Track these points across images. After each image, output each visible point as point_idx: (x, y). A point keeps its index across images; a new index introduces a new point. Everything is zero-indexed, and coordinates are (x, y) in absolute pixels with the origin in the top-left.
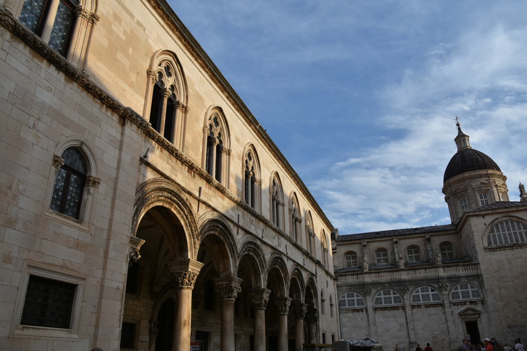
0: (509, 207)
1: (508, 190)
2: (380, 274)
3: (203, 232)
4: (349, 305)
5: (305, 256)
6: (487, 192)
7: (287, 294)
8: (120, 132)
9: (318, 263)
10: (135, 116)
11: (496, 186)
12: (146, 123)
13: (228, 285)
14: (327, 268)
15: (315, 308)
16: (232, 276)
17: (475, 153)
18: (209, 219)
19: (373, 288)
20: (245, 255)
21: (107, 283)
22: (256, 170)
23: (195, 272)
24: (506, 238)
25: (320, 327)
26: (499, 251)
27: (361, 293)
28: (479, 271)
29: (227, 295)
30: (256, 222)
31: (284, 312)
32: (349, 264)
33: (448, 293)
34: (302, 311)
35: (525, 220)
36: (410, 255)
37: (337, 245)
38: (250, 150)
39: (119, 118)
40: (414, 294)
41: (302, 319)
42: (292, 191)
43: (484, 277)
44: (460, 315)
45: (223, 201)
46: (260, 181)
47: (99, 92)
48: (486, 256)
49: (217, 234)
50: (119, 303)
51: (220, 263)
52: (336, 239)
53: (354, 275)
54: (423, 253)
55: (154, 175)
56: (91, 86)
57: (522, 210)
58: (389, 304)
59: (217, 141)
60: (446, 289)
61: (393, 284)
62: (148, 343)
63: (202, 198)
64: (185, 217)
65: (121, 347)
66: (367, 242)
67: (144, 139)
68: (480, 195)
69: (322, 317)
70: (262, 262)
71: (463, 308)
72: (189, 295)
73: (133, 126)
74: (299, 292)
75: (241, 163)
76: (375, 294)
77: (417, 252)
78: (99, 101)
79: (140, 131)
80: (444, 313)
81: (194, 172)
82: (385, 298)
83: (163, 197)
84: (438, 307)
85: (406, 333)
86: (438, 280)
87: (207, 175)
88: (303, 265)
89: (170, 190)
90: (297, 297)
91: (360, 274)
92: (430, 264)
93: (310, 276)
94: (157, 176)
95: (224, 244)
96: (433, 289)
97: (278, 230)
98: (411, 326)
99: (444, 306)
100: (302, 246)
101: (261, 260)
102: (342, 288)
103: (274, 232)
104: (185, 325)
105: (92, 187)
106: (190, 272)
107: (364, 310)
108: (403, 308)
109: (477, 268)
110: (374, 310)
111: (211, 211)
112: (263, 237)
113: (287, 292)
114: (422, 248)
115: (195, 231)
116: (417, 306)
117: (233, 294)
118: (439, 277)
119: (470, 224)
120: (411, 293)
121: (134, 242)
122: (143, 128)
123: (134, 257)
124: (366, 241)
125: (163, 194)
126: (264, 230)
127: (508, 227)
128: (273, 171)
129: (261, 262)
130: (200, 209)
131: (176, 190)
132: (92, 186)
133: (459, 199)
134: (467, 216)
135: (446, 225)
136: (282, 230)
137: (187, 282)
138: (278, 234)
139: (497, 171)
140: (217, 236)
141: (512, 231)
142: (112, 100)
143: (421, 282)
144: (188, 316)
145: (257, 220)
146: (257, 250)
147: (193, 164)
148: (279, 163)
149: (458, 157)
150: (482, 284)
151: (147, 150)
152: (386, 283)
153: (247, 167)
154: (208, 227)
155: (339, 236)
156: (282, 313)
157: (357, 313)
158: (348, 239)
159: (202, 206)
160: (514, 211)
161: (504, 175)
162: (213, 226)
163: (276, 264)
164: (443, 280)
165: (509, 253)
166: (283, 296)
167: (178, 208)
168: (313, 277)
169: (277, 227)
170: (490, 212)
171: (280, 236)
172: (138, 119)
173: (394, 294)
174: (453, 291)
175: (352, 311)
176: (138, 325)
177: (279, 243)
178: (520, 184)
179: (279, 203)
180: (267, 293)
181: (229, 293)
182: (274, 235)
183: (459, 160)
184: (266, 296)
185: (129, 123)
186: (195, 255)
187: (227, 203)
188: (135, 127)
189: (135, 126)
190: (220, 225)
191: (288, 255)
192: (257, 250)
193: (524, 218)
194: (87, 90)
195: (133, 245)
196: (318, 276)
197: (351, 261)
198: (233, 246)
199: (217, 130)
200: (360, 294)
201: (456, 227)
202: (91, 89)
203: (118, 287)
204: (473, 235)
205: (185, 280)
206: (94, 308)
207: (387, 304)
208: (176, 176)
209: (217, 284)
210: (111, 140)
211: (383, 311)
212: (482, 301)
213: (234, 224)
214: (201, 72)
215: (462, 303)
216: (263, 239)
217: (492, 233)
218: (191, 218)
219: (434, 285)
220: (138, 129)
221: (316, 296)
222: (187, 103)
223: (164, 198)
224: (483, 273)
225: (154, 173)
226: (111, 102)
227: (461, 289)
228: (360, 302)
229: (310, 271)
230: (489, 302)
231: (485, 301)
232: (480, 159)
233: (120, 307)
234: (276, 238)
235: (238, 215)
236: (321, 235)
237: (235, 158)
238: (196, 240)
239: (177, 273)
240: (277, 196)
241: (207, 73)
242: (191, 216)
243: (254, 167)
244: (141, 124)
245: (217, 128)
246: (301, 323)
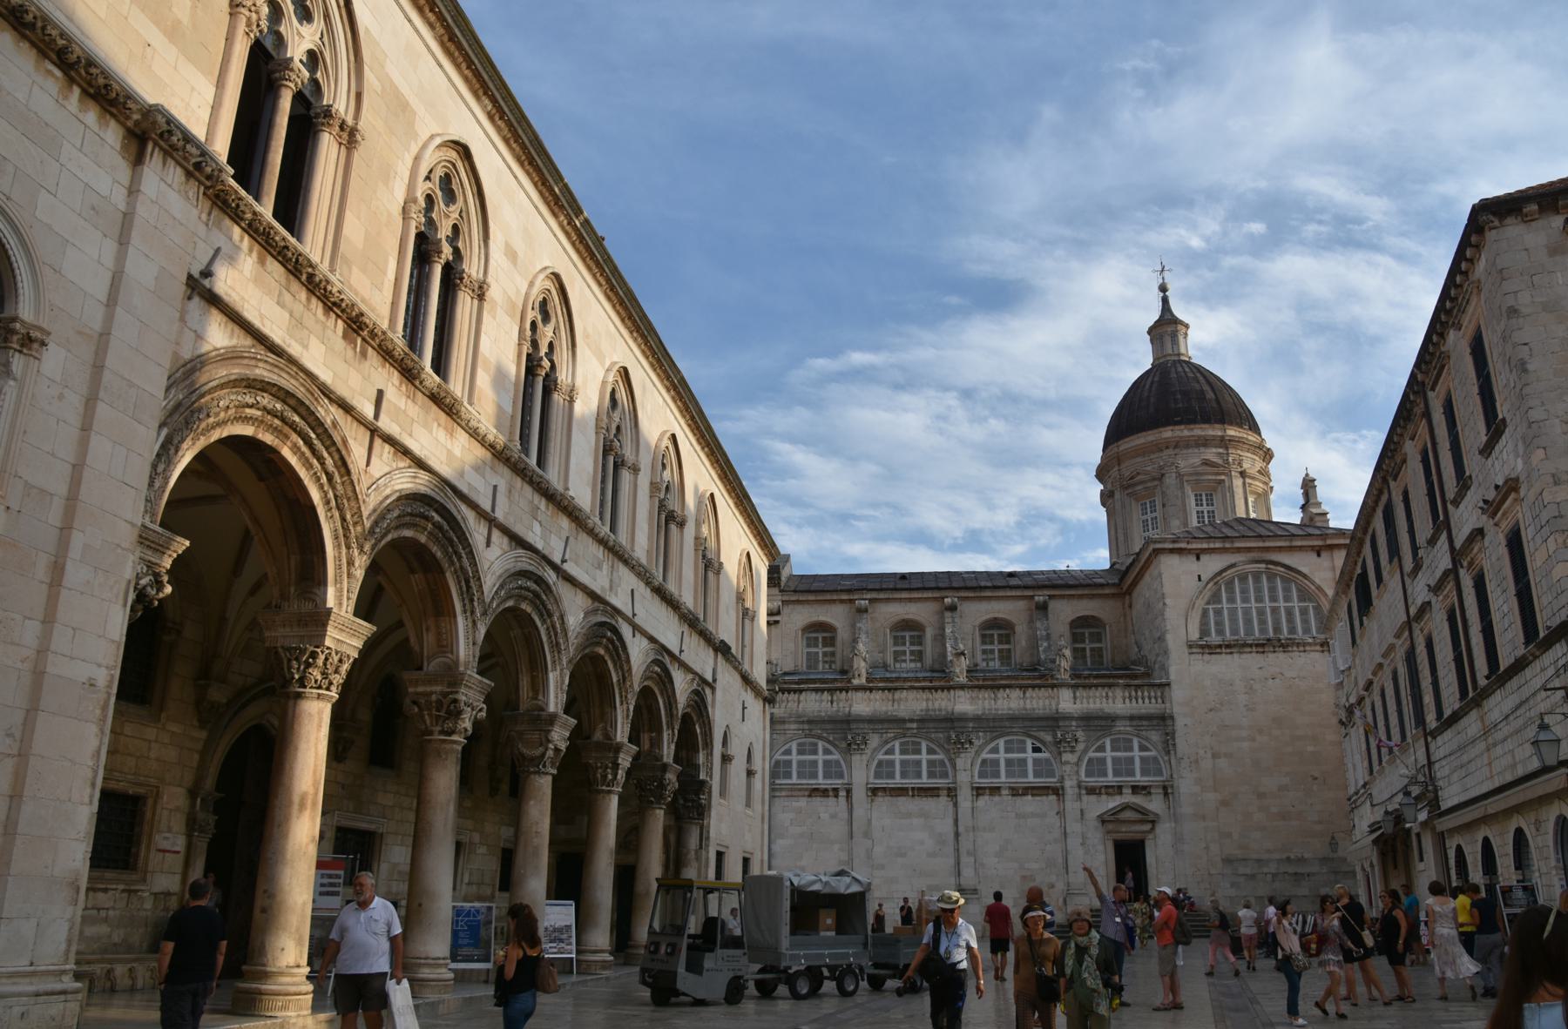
0: (1269, 536)
1: (1272, 488)
2: (898, 695)
3: (378, 530)
4: (799, 777)
5: (686, 626)
6: (1215, 490)
7: (622, 733)
8: (126, 184)
9: (722, 649)
10: (180, 136)
11: (1243, 474)
12: (214, 165)
13: (445, 695)
14: (746, 667)
15: (701, 778)
16: (462, 669)
17: (1198, 375)
18: (400, 491)
19: (874, 731)
20: (505, 609)
21: (56, 667)
22: (562, 356)
23: (344, 649)
24: (1248, 621)
25: (712, 834)
26: (1226, 653)
28: (1168, 705)
29: (442, 726)
30: (549, 513)
31: (608, 786)
32: (812, 660)
33: (1076, 760)
34: (662, 786)
35: (1305, 576)
36: (985, 647)
37: (783, 601)
38: (549, 291)
39: (124, 138)
40: (985, 755)
42: (665, 432)
43: (1180, 722)
44: (1103, 822)
45: (449, 442)
46: (572, 390)
47: (61, 42)
48: (1190, 665)
49: (423, 539)
50: (93, 729)
51: (427, 630)
52: (782, 584)
53: (823, 690)
54: (1024, 643)
55: (232, 335)
56: (30, 17)
57: (1301, 547)
58: (914, 778)
59: (447, 251)
60: (1073, 747)
61: (931, 725)
62: (180, 858)
63: (385, 424)
64: (324, 479)
65: (91, 866)
66: (871, 600)
67: (204, 217)
68: (1196, 495)
69: (720, 804)
70: (556, 635)
71: (1113, 803)
72: (321, 719)
73: (172, 169)
74: (660, 732)
75: (516, 329)
76: (876, 750)
77: (1005, 639)
78: (58, 73)
79: (193, 189)
80: (1061, 814)
81: (364, 339)
82: (903, 763)
83: (258, 409)
84: (1047, 795)
85: (952, 861)
86: (1054, 721)
87: (406, 354)
88: (677, 653)
89: (280, 388)
90: (652, 745)
91: (841, 690)
92: (1038, 675)
93: (695, 686)
94: (243, 341)
95: (442, 572)
96: (1039, 745)
97: (611, 543)
98: (965, 844)
99: (1063, 795)
100: (680, 596)
101: (554, 627)
102: (787, 726)
103: (601, 548)
104: (302, 806)
105: (17, 354)
106: (328, 648)
107: (843, 793)
108: (952, 793)
109: (1162, 697)
111: (410, 467)
112: (564, 561)
113: (623, 727)
114: (1021, 630)
115: (355, 524)
116: (991, 788)
117: (460, 722)
118: (1057, 713)
119: (1160, 575)
120: (978, 753)
121: (153, 542)
122: (203, 179)
123: (149, 589)
124: (869, 596)
125: (258, 398)
126: (571, 539)
127: (1258, 590)
128: (614, 363)
129: (552, 633)
130: (374, 459)
131: (300, 392)
132: (20, 352)
133: (1137, 500)
134: (1154, 550)
135: (1096, 572)
136: (624, 543)
137: (319, 678)
138: (610, 555)
139: (1250, 433)
140: (424, 547)
141: (1268, 604)
142: (102, 73)
143: (1007, 724)
144: (315, 780)
145: (551, 506)
146: (544, 597)
147: (362, 314)
148: (635, 340)
149: (1152, 383)
150: (1170, 742)
151: (212, 252)
152: (911, 721)
153: (535, 344)
154: (395, 515)
155: (791, 577)
156: (604, 788)
157: (822, 799)
158: (816, 586)
159: (383, 448)
160: (1280, 549)
161: (1268, 445)
162: (411, 515)
163: (598, 644)
164: (1067, 723)
165: (1251, 662)
166: (610, 739)
167: (304, 449)
168: (703, 689)
169: (612, 535)
170: (1218, 545)
171: (616, 560)
172: (188, 146)
173: (930, 751)
174: (1091, 754)
175: (807, 793)
176: (150, 802)
177: (611, 580)
178: (1307, 475)
179: (623, 463)
180: (564, 726)
181: (447, 719)
182: (601, 556)
183: (1154, 389)
184: (559, 736)
185: (157, 157)
186: (348, 599)
187: (463, 446)
188: (176, 174)
189: (179, 170)
190: (434, 514)
191: (637, 620)
192: (544, 597)
193: (1304, 570)
194: (15, 29)
195: (150, 553)
196: (719, 686)
197: (820, 650)
198: (470, 580)
199: (447, 216)
201: (1122, 579)
202: (32, 26)
203: (90, 679)
204: (1164, 604)
205: (310, 670)
206: (8, 741)
207: (909, 778)
208: (306, 347)
209: (411, 690)
210: (93, 209)
211: (895, 799)
212: (1165, 788)
213: (478, 513)
214: (410, 21)
215: (1111, 790)
216: (566, 566)
217: (1214, 603)
218: (343, 483)
219: (1042, 735)
220: (188, 180)
221: (709, 744)
222: (357, 116)
223: (259, 413)
224: (1177, 710)
225: (233, 330)
226: (101, 81)
227: (1113, 750)
228: (832, 769)
229: (699, 671)
230: (1181, 791)
231: (1172, 787)
232: (1210, 395)
233: (94, 743)
234: (605, 566)
235: (495, 487)
236: (739, 570)
237: (500, 312)
238: (356, 552)
239: (289, 649)
240: (619, 441)
241: (431, 26)
242: (346, 478)
243: (556, 343)
244: (198, 166)
245: (450, 209)
246: (658, 819)
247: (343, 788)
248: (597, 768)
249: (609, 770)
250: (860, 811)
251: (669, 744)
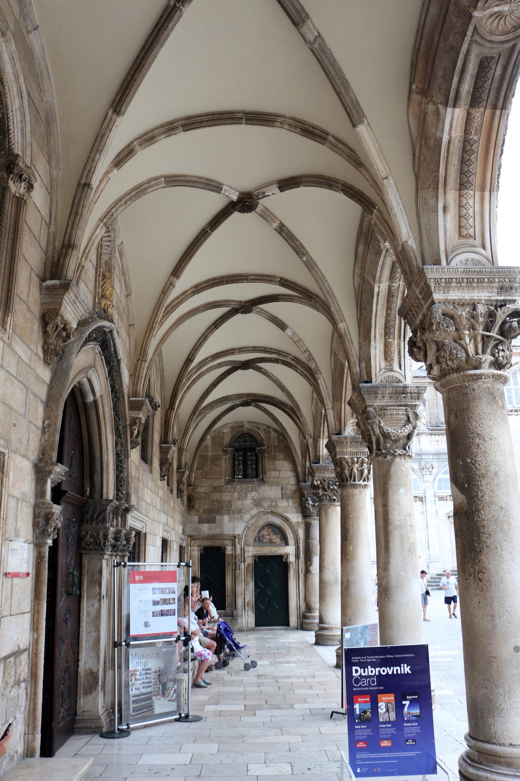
31: (364, 480)
51: (445, 209)
60: (431, 472)
99: (425, 501)
118: (421, 451)
164: (427, 457)
248: (353, 463)
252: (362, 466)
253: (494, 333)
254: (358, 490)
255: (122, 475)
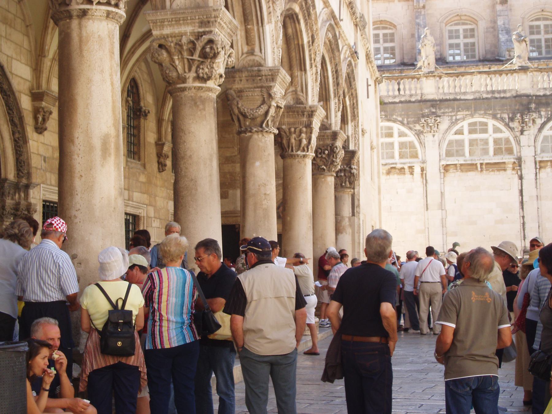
13: (199, 36)
27: (411, 126)
31: (304, 150)
41: (332, 175)
107: (417, 170)
110: (442, 171)
117: (214, 65)
166: (302, 103)
173: (497, 130)
200: (410, 129)
247: (45, 161)
249: (303, 135)
250: (434, 186)
251: (336, 112)
252: (300, 135)
253: (196, 57)
254: (297, 160)
255: (21, 158)
